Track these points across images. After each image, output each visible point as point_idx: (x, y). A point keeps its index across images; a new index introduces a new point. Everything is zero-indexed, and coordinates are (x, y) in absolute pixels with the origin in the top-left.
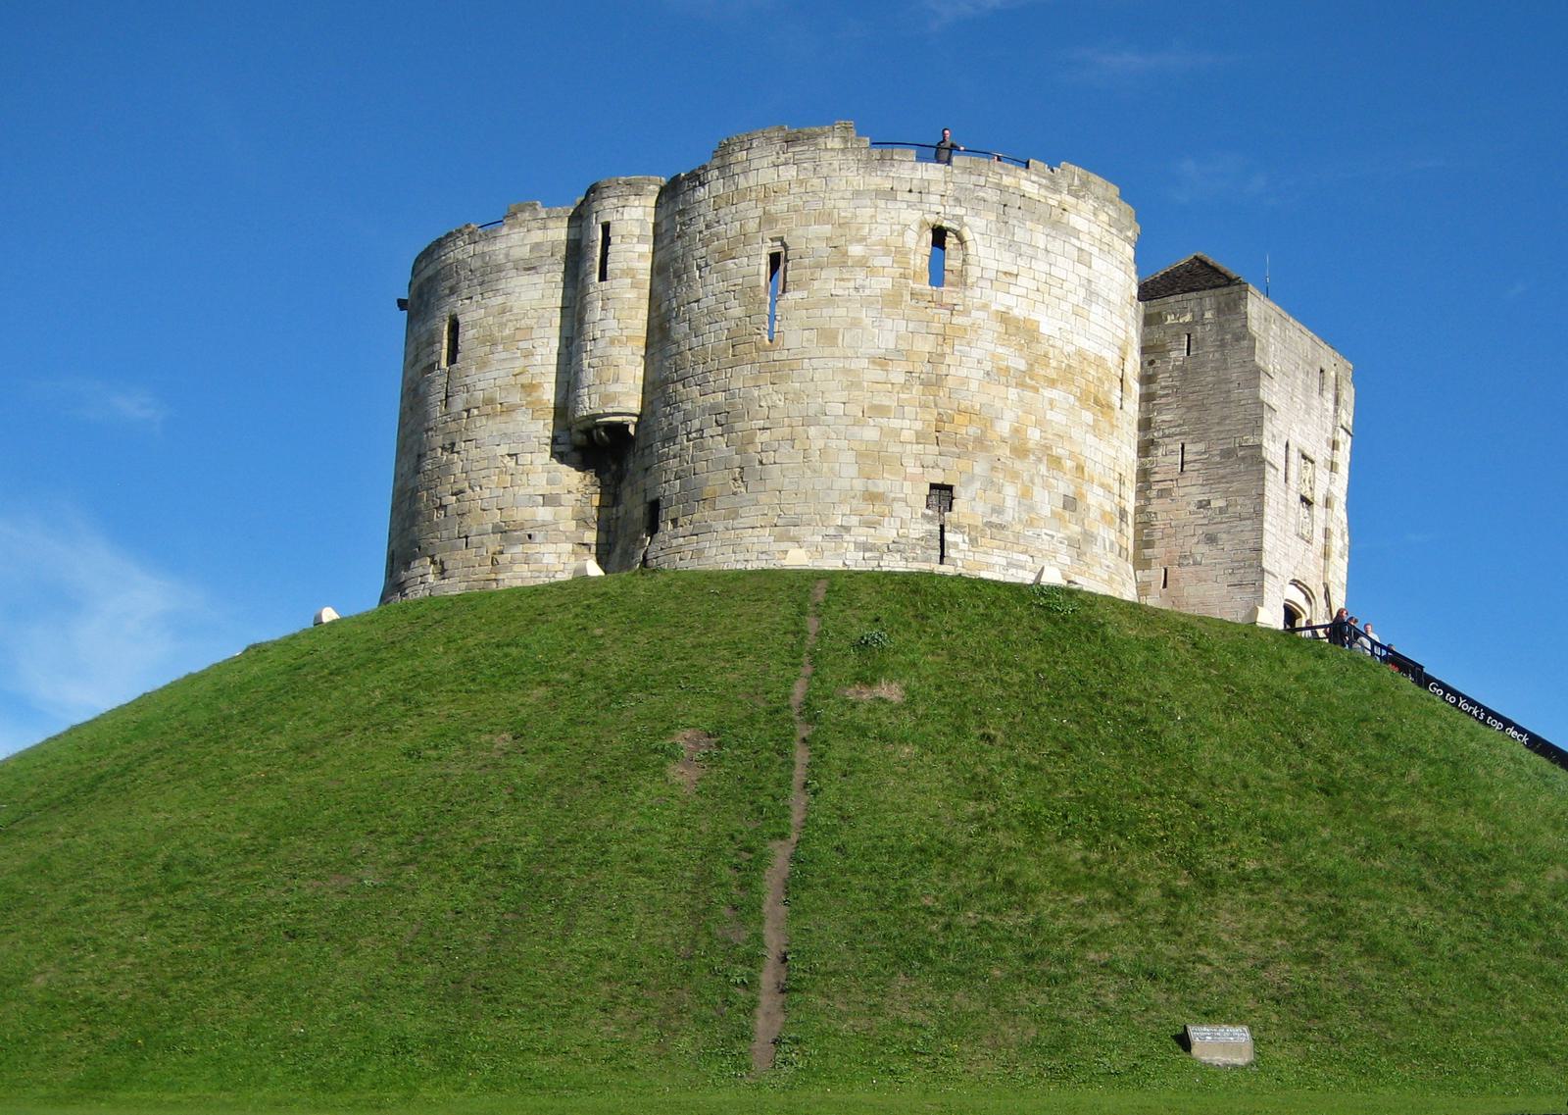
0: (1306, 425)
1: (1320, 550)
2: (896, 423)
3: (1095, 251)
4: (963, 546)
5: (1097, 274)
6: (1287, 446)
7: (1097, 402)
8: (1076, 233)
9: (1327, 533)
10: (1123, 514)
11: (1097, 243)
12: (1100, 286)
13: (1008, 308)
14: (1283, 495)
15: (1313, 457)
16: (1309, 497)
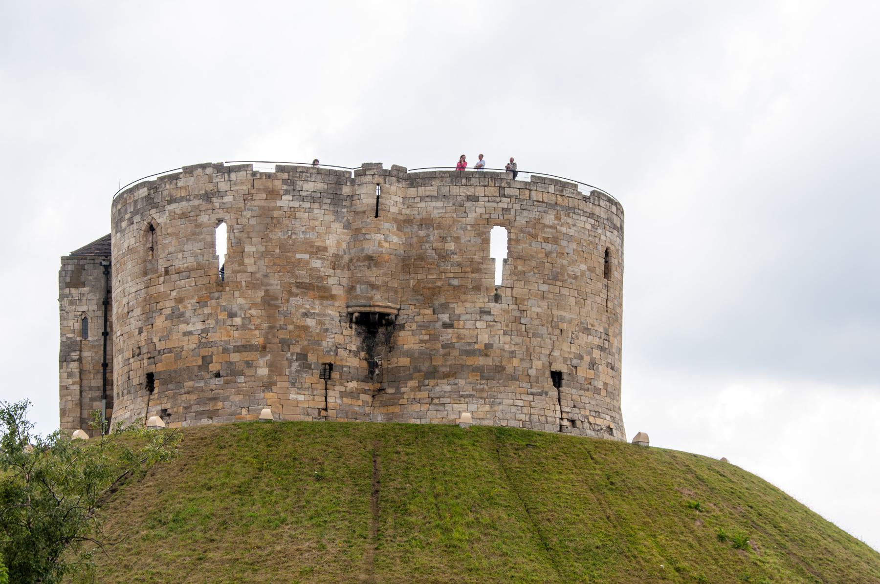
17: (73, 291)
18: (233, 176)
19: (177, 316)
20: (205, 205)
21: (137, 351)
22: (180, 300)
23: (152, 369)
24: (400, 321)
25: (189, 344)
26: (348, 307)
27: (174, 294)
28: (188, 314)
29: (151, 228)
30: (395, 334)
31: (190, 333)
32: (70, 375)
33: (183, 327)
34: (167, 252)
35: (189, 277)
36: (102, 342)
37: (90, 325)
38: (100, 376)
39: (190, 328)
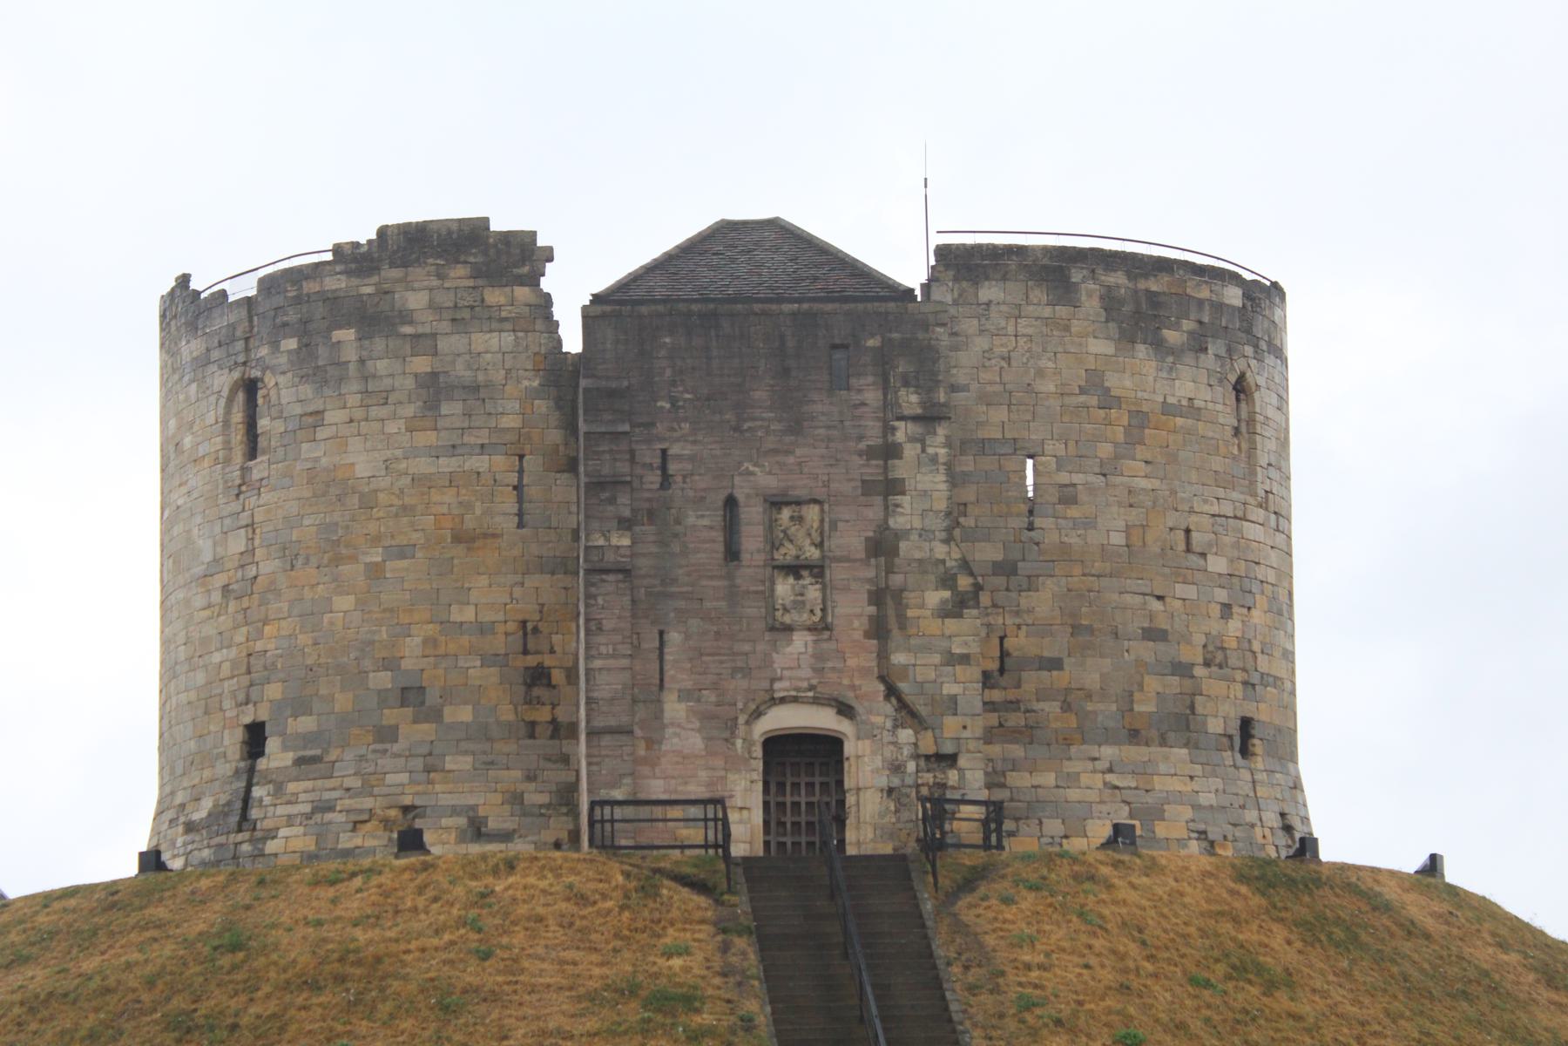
0: (788, 452)
1: (861, 625)
2: (217, 658)
3: (445, 326)
4: (267, 800)
5: (449, 358)
6: (731, 503)
7: (457, 539)
8: (406, 317)
10: (538, 677)
11: (447, 315)
12: (461, 371)
13: (317, 460)
14: (726, 583)
15: (820, 493)
16: (813, 553)
23: (1249, 710)
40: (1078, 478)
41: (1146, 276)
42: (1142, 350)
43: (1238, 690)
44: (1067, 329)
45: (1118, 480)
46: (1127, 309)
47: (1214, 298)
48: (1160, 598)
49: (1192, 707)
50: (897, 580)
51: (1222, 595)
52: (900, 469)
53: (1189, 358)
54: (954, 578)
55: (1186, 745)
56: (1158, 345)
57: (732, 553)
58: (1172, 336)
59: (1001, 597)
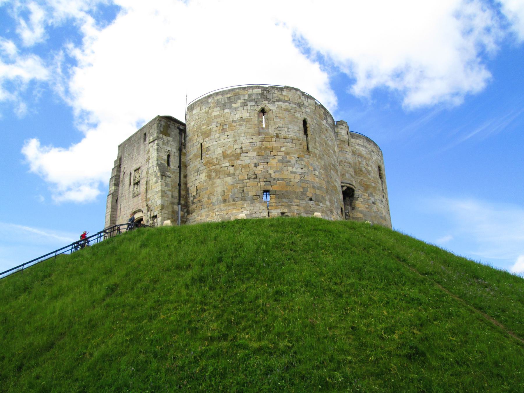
6: (131, 173)
9: (147, 183)
17: (164, 137)
18: (309, 100)
19: (285, 162)
20: (298, 109)
21: (254, 176)
22: (287, 153)
24: (356, 196)
25: (295, 179)
26: (342, 183)
27: (283, 149)
28: (293, 162)
29: (263, 111)
30: (354, 201)
31: (295, 173)
32: (167, 185)
33: (290, 169)
34: (277, 126)
35: (292, 143)
36: (178, 172)
37: (172, 160)
38: (177, 190)
39: (294, 170)
40: (210, 145)
41: (227, 94)
42: (226, 111)
43: (262, 184)
44: (208, 112)
45: (220, 142)
46: (223, 102)
47: (249, 93)
48: (233, 166)
49: (243, 191)
50: (149, 178)
51: (255, 161)
52: (150, 154)
53: (241, 108)
54: (157, 174)
55: (241, 200)
56: (231, 108)
57: (130, 185)
58: (234, 105)
59: (197, 178)
